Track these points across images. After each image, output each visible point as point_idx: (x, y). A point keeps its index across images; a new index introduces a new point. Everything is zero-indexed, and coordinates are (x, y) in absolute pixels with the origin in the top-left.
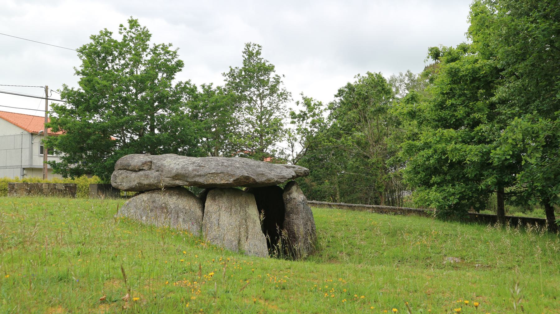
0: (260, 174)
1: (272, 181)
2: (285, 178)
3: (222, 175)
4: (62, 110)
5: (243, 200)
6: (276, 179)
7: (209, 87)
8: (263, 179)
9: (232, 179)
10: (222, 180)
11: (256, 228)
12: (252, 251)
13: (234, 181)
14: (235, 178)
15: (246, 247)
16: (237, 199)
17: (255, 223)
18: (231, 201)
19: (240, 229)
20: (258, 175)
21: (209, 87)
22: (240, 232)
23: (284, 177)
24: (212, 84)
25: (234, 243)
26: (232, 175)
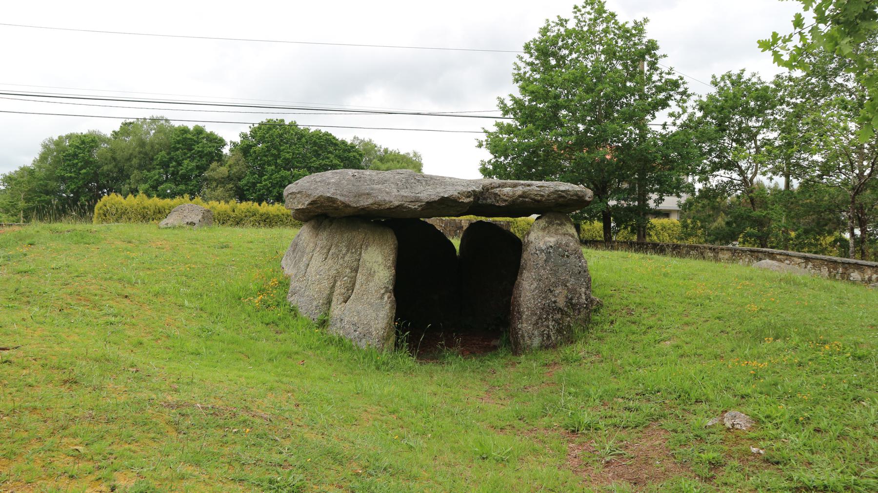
0: (364, 194)
1: (388, 206)
2: (421, 201)
3: (299, 195)
4: (509, 130)
5: (358, 236)
6: (397, 203)
7: (740, 76)
8: (365, 202)
9: (307, 203)
10: (299, 203)
11: (371, 284)
12: (346, 319)
13: (309, 204)
14: (310, 201)
15: (336, 312)
16: (345, 236)
17: (371, 274)
18: (333, 237)
19: (335, 282)
20: (360, 195)
21: (740, 76)
22: (333, 286)
23: (417, 200)
24: (744, 70)
25: (315, 303)
26: (309, 196)
